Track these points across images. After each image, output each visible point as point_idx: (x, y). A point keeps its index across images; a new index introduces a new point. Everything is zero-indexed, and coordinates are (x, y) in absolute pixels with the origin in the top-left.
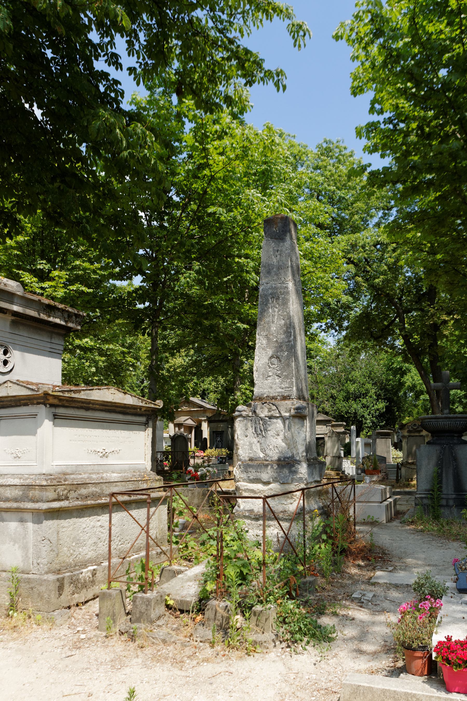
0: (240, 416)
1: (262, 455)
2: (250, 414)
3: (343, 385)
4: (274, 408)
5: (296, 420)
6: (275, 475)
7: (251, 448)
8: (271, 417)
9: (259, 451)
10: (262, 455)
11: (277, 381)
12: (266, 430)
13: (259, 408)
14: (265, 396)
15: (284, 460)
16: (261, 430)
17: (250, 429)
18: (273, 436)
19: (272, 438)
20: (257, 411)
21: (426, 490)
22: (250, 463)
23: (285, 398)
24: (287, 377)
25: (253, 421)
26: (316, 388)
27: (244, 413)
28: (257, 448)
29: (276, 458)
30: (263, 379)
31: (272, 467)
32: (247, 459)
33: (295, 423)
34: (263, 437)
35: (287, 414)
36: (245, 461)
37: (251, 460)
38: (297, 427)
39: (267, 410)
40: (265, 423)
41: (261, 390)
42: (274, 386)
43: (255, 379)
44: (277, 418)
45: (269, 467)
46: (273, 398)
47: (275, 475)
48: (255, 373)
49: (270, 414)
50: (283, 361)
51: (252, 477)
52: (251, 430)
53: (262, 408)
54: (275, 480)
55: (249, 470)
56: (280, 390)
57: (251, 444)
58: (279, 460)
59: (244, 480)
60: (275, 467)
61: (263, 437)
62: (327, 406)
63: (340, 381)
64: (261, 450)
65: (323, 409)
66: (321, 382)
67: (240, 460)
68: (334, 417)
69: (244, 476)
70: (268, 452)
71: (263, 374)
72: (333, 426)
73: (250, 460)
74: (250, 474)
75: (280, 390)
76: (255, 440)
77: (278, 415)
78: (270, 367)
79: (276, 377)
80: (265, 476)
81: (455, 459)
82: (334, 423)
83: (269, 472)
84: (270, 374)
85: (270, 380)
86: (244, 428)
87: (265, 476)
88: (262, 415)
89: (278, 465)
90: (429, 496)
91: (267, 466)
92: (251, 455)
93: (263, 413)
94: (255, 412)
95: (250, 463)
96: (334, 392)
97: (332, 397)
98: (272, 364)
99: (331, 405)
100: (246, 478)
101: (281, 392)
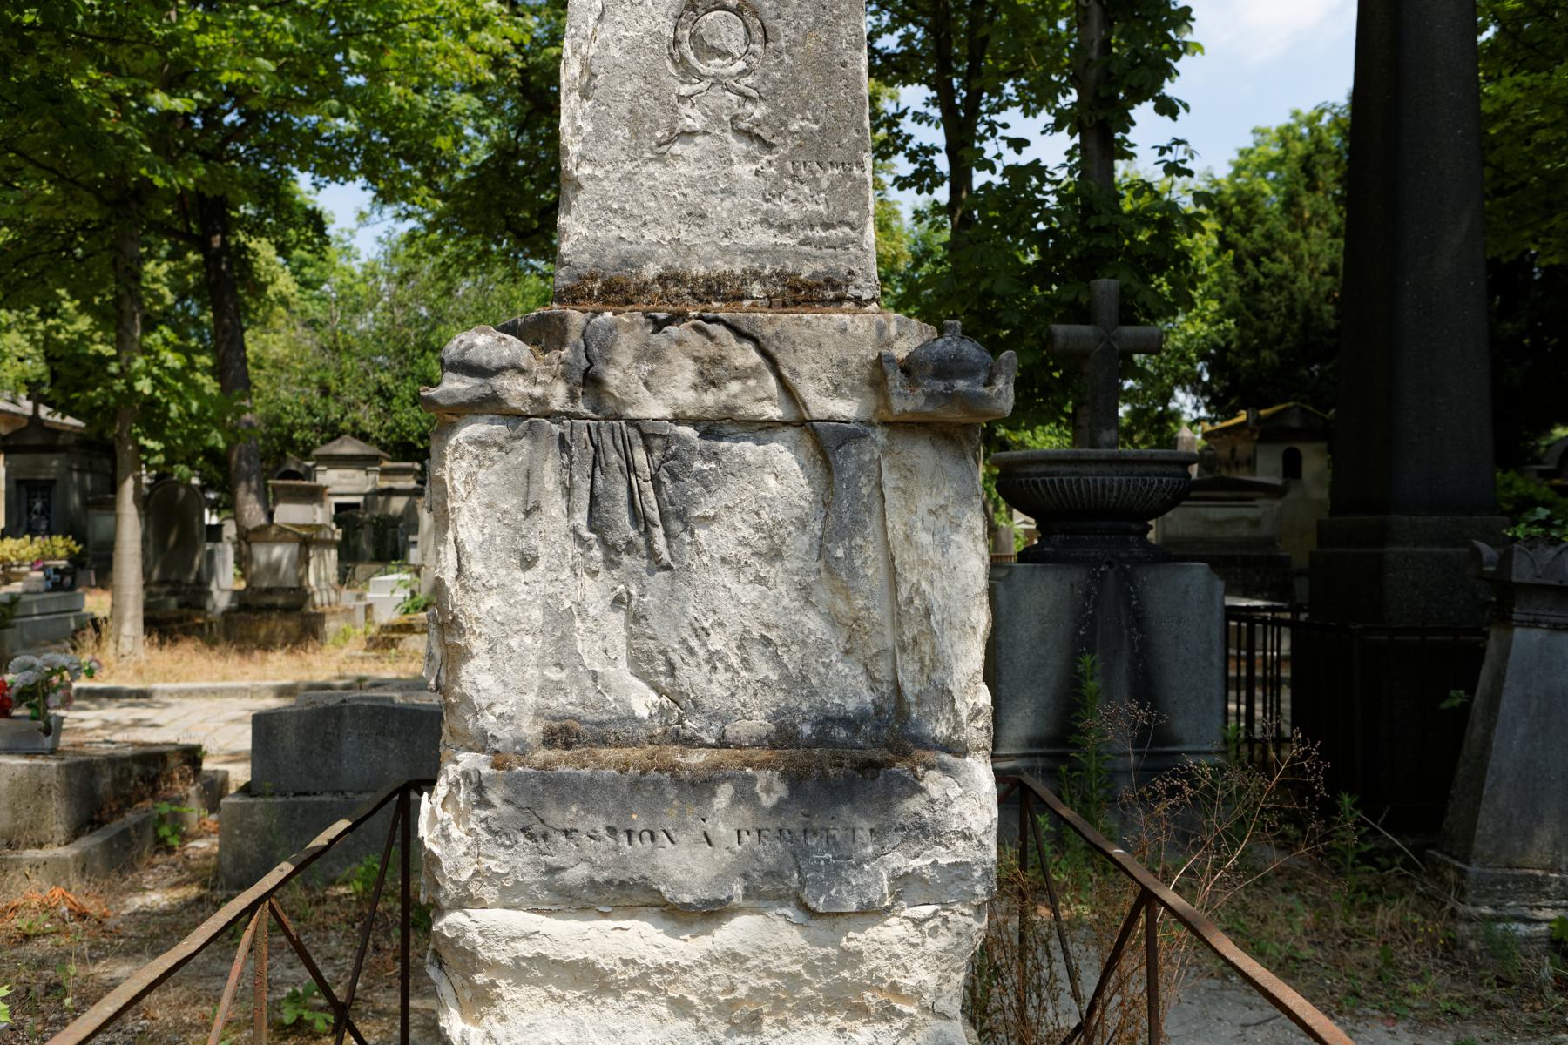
0: (490, 405)
1: (643, 702)
2: (559, 396)
3: (414, 363)
4: (748, 356)
5: (922, 454)
6: (770, 853)
7: (562, 651)
8: (713, 427)
9: (621, 673)
10: (643, 702)
11: (744, 171)
12: (678, 516)
13: (624, 354)
14: (651, 270)
15: (822, 739)
16: (639, 518)
17: (555, 507)
18: (738, 566)
19: (726, 576)
20: (613, 377)
21: (1032, 742)
22: (564, 762)
23: (801, 293)
24: (816, 148)
25: (582, 453)
26: (333, 366)
27: (515, 389)
28: (604, 644)
29: (757, 723)
30: (634, 150)
31: (746, 793)
32: (532, 730)
33: (909, 471)
34: (656, 564)
35: (846, 408)
36: (522, 749)
37: (561, 735)
38: (925, 502)
39: (687, 372)
40: (672, 463)
41: (619, 228)
42: (721, 208)
43: (572, 145)
44: (762, 429)
45: (723, 796)
46: (715, 288)
47: (770, 853)
48: (570, 104)
49: (710, 398)
50: (785, 33)
51: (577, 874)
52: (559, 519)
53: (655, 355)
54: (767, 890)
55: (555, 817)
56: (765, 237)
57: (560, 621)
58: (782, 736)
59: (511, 896)
60: (770, 789)
61: (656, 564)
62: (366, 417)
63: (403, 351)
64: (640, 663)
65: (355, 424)
66: (348, 349)
67: (481, 743)
68: (384, 447)
69: (517, 861)
70: (692, 676)
71: (635, 119)
72: (385, 473)
73: (550, 739)
74: (560, 853)
75: (765, 237)
76: (593, 592)
77: (774, 412)
78: (687, 72)
79: (738, 146)
80: (685, 865)
81: (1138, 619)
82: (387, 464)
83: (723, 830)
84: (692, 118)
85: (688, 160)
86: (511, 503)
87: (685, 865)
88: (653, 409)
89: (795, 779)
90: (1040, 763)
91: (701, 786)
92: (560, 703)
93: (661, 389)
94: (590, 382)
95: (564, 762)
96: (385, 378)
97: (380, 392)
98: (707, 51)
99: (378, 416)
100: (529, 876)
101: (775, 252)
